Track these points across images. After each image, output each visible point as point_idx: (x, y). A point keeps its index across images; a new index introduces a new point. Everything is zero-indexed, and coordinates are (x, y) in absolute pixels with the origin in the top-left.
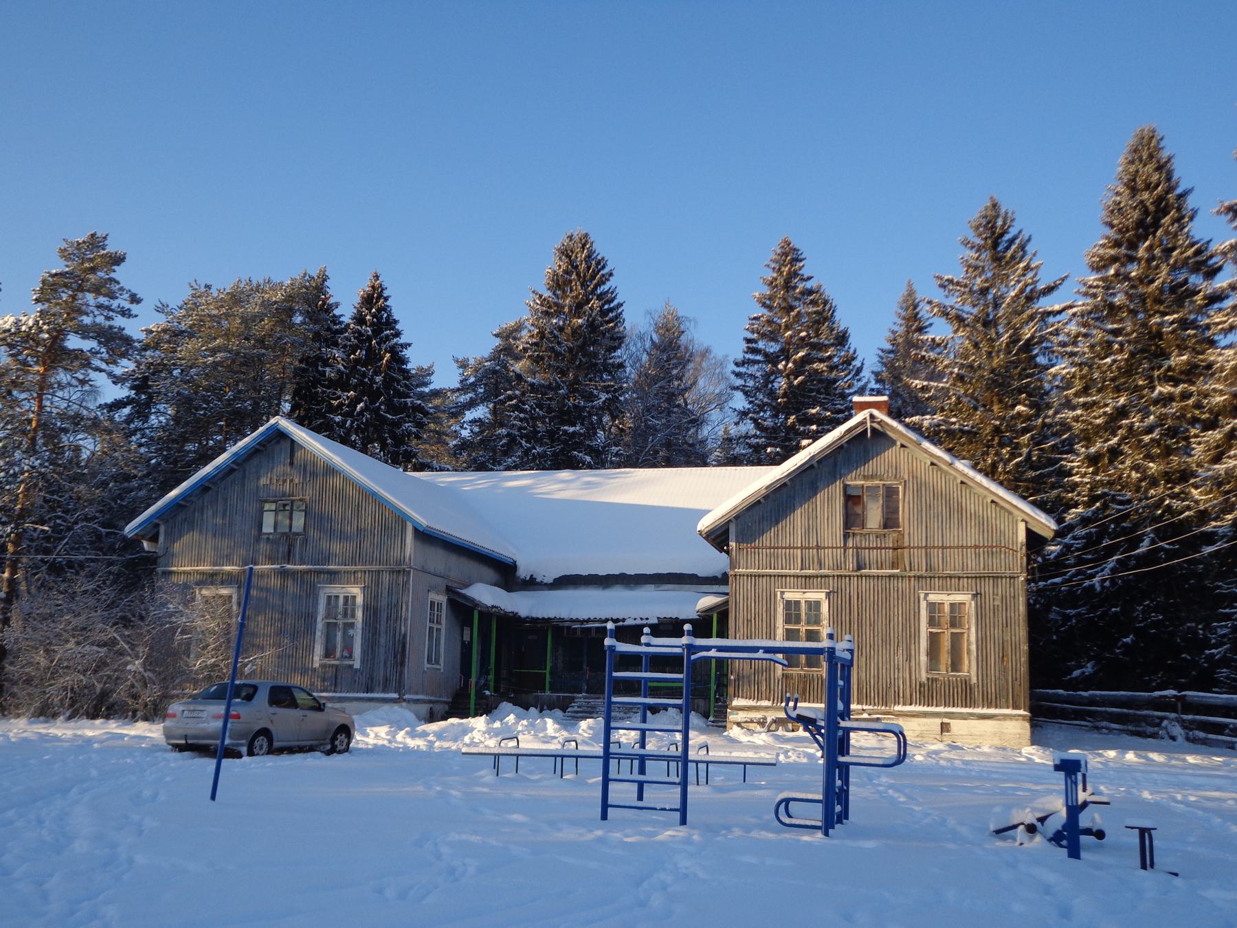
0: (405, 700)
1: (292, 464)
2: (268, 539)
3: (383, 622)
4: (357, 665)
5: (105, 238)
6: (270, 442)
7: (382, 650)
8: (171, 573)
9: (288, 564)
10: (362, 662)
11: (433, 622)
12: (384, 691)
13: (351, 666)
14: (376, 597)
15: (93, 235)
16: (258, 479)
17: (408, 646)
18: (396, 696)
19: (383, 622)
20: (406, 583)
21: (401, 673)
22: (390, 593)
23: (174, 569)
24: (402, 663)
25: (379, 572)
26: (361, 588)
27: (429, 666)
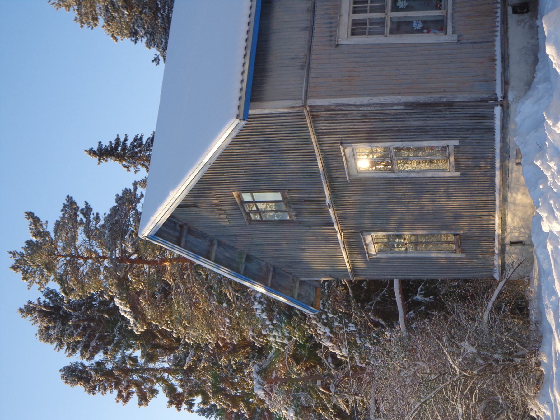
0: (505, 97)
1: (195, 206)
2: (296, 216)
3: (387, 124)
4: (456, 142)
5: (14, 254)
6: (175, 223)
7: (432, 122)
8: (354, 269)
9: (325, 201)
10: (451, 138)
11: (382, 22)
12: (492, 117)
13: (456, 147)
14: (356, 132)
15: (14, 268)
16: (224, 227)
17: (422, 98)
18: (498, 110)
19: (387, 124)
20: (328, 108)
21: (464, 105)
22: (346, 121)
23: (349, 270)
24: (450, 105)
25: (317, 133)
26: (344, 149)
27: (450, 29)
